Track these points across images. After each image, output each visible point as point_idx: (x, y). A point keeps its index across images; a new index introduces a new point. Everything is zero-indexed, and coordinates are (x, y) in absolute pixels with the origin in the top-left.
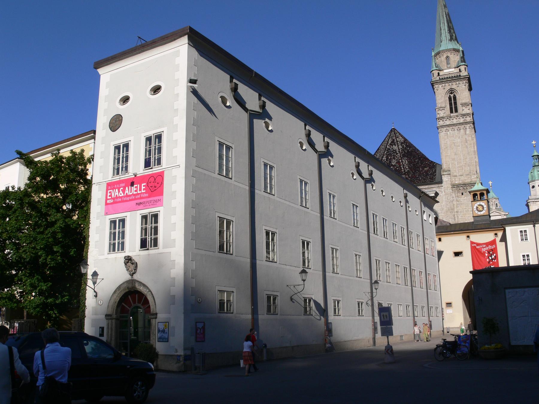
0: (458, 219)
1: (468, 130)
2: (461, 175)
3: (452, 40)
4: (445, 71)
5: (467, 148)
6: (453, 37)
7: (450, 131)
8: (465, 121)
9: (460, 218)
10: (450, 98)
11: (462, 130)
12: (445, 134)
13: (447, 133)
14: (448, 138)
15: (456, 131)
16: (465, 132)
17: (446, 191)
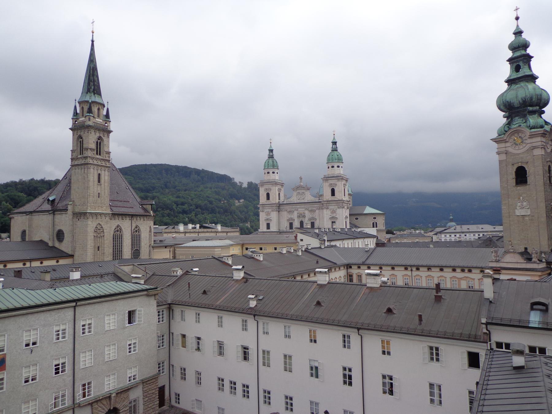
0: (75, 238)
1: (86, 169)
2: (79, 205)
3: (89, 93)
4: (81, 119)
5: (84, 184)
6: (91, 89)
7: (77, 170)
8: (85, 163)
9: (76, 238)
10: (80, 142)
11: (83, 170)
12: (74, 171)
13: (75, 171)
14: (75, 175)
15: (80, 170)
16: (84, 171)
17: (69, 217)
